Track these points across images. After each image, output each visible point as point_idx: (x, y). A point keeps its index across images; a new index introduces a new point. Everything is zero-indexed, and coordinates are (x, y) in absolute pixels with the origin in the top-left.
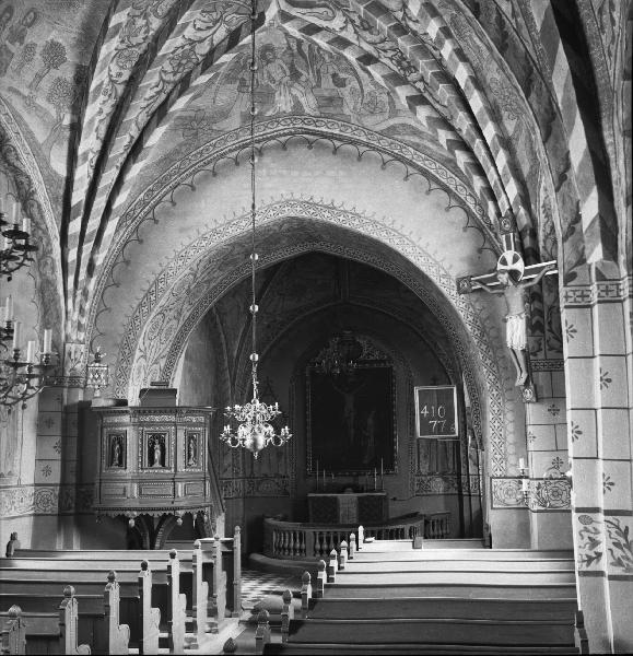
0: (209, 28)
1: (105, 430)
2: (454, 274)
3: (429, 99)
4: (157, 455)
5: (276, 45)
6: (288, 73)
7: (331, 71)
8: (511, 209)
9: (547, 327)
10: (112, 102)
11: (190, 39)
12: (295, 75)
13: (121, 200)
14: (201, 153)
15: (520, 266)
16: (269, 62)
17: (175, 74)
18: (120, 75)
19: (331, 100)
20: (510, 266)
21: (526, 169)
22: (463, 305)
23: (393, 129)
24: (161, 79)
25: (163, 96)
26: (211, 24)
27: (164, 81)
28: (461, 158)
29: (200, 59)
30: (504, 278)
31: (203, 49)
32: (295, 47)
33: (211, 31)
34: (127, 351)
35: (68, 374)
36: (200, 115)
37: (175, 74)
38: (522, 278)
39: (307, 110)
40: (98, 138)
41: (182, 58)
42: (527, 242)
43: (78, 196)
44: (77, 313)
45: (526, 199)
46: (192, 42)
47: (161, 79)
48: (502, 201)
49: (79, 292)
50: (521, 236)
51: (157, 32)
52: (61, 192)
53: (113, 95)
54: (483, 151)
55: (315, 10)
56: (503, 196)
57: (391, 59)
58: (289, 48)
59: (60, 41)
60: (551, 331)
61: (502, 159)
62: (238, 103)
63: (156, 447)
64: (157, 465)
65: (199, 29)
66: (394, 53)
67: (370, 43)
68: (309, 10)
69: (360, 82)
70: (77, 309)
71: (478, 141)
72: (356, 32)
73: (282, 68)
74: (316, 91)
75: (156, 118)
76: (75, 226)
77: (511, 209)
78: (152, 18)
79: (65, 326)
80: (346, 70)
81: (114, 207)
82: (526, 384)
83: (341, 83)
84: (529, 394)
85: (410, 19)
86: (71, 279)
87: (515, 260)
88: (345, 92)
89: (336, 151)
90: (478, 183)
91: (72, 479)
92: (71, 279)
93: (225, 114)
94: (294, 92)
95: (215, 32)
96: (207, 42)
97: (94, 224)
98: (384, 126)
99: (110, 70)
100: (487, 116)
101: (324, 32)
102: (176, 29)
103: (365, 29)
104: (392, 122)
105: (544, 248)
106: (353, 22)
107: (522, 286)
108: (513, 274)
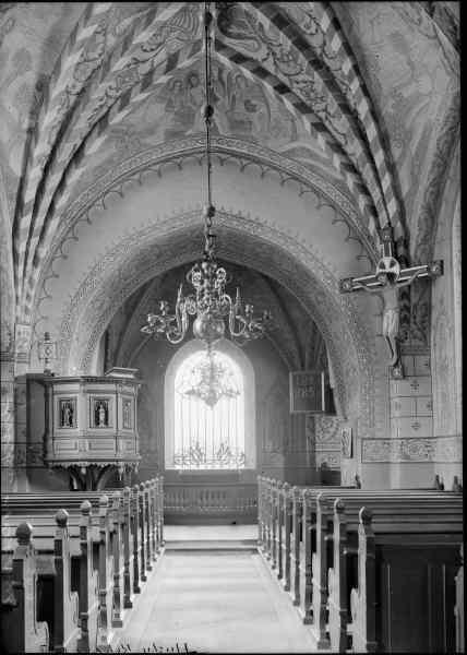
0: (152, 50)
1: (56, 397)
2: (337, 276)
3: (330, 128)
4: (102, 417)
7: (244, 98)
8: (389, 223)
9: (412, 320)
10: (64, 111)
13: (62, 202)
15: (396, 269)
20: (388, 270)
21: (405, 189)
22: (344, 302)
23: (293, 151)
24: (106, 94)
25: (105, 110)
26: (154, 47)
28: (350, 180)
29: (141, 77)
30: (383, 279)
34: (66, 333)
35: (17, 351)
38: (397, 279)
40: (49, 142)
42: (401, 251)
43: (30, 195)
44: (25, 298)
45: (402, 214)
46: (137, 62)
47: (106, 94)
48: (382, 216)
49: (26, 280)
50: (395, 246)
52: (16, 191)
54: (371, 174)
56: (384, 212)
57: (301, 90)
60: (415, 323)
61: (386, 181)
63: (100, 413)
64: (102, 425)
65: (145, 51)
67: (285, 75)
70: (25, 295)
71: (368, 165)
72: (275, 63)
75: (97, 130)
76: (25, 222)
77: (389, 223)
78: (109, 36)
79: (16, 310)
81: (57, 207)
82: (396, 365)
83: (250, 108)
84: (397, 372)
86: (21, 268)
87: (392, 265)
90: (362, 202)
91: (23, 439)
92: (21, 268)
93: (151, 132)
96: (148, 63)
97: (40, 221)
100: (378, 144)
101: (248, 62)
104: (294, 145)
105: (416, 256)
106: (274, 54)
107: (398, 285)
108: (391, 276)
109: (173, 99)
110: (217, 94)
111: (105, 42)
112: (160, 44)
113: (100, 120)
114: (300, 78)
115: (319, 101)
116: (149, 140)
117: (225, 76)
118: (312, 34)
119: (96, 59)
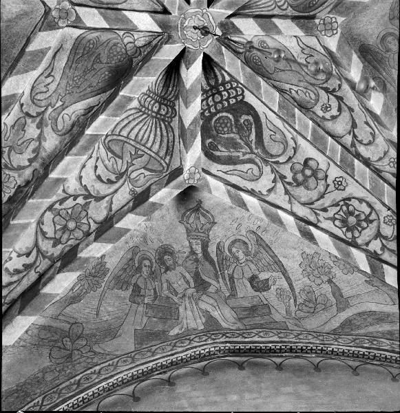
0: (110, 182)
5: (176, 247)
6: (192, 285)
12: (201, 285)
14: (79, 383)
16: (167, 269)
17: (57, 242)
19: (253, 310)
23: (348, 323)
24: (36, 245)
25: (33, 276)
26: (113, 178)
27: (39, 251)
29: (93, 226)
31: (98, 212)
32: (198, 249)
37: (57, 242)
39: (224, 325)
41: (71, 218)
47: (36, 245)
51: (49, 156)
55: (239, 167)
57: (333, 219)
58: (193, 252)
62: (131, 318)
65: (99, 177)
67: (304, 204)
68: (231, 167)
69: (288, 279)
72: (287, 192)
73: (185, 277)
74: (232, 302)
75: (18, 305)
78: (48, 130)
80: (268, 268)
85: (360, 142)
88: (271, 296)
89: (279, 367)
93: (111, 332)
94: (203, 306)
95: (116, 191)
96: (104, 203)
98: (335, 324)
102: (82, 142)
103: (299, 185)
104: (344, 316)
106: (283, 177)
109: (141, 283)
110: (207, 279)
111: (40, 138)
112: (120, 175)
113: (23, 294)
114: (327, 201)
115: (364, 224)
116: (110, 346)
117: (212, 250)
118: (334, 118)
119: (20, 168)
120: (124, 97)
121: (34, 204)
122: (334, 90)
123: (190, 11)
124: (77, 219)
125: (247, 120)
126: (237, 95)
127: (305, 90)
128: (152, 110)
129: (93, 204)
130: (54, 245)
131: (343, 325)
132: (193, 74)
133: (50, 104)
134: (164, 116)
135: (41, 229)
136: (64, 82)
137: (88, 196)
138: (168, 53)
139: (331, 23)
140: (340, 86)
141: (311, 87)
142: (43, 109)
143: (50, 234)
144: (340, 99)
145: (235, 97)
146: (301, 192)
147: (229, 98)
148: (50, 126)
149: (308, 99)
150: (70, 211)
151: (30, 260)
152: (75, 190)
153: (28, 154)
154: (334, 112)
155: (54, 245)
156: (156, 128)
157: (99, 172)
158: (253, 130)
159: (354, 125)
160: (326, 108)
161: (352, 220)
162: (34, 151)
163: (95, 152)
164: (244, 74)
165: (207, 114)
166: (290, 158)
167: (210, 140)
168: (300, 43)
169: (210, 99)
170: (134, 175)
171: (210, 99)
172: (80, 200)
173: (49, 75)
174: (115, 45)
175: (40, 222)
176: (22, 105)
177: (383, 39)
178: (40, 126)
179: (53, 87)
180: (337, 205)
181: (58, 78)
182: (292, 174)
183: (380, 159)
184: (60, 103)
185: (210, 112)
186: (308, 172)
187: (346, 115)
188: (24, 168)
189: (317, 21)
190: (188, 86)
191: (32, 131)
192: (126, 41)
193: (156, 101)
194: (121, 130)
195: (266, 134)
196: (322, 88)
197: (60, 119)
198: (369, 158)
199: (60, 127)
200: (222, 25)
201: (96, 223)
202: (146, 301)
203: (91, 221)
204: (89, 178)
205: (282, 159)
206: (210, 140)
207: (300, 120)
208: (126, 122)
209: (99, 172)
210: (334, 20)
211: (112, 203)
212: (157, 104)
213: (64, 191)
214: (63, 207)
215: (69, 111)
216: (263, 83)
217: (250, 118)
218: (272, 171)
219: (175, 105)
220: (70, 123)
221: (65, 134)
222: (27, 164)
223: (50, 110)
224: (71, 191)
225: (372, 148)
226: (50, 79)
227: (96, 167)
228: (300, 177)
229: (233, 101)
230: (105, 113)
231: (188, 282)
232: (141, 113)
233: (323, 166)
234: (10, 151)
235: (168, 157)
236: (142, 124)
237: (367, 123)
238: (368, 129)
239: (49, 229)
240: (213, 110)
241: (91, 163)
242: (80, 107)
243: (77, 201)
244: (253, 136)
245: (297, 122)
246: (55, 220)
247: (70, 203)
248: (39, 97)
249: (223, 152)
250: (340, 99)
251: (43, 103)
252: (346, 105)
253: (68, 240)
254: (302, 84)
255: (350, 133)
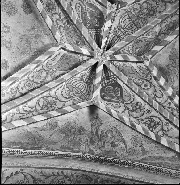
0: (66, 98)
5: (86, 129)
6: (89, 141)
7: (111, 142)
11: (57, 96)
12: (92, 142)
16: (81, 134)
17: (42, 109)
18: (22, 89)
24: (35, 107)
26: (67, 97)
27: (36, 109)
32: (94, 132)
33: (66, 100)
36: (40, 138)
41: (49, 103)
47: (35, 107)
53: (14, 95)
55: (112, 103)
57: (145, 123)
58: (92, 132)
59: (10, 63)
62: (61, 142)
65: (62, 95)
66: (147, 120)
67: (135, 118)
68: (110, 103)
69: (125, 145)
72: (129, 113)
73: (86, 138)
74: (102, 149)
78: (49, 76)
80: (118, 140)
85: (157, 97)
88: (117, 149)
95: (67, 101)
96: (62, 103)
99: (20, 83)
103: (134, 111)
104: (144, 157)
106: (128, 108)
109: (69, 134)
110: (94, 140)
111: (46, 77)
112: (70, 97)
114: (144, 117)
115: (157, 125)
117: (99, 133)
118: (148, 89)
119: (37, 83)
120: (75, 70)
121: (37, 91)
122: (149, 80)
123: (101, 51)
124: (51, 104)
125: (118, 89)
126: (115, 80)
127: (139, 80)
128: (85, 81)
129: (58, 102)
130: (41, 109)
131: (142, 159)
132: (100, 69)
133: (52, 69)
134: (89, 83)
135: (38, 103)
136: (58, 64)
137: (57, 99)
138: (93, 62)
139: (147, 57)
140: (151, 79)
141: (141, 79)
142: (49, 69)
143: (41, 105)
144: (151, 83)
145: (114, 81)
146: (135, 114)
147: (112, 81)
148: (50, 75)
149: (140, 83)
150: (49, 101)
151: (32, 110)
152: (53, 95)
153: (41, 80)
154: (149, 87)
155: (41, 109)
156: (86, 86)
157: (62, 93)
158: (120, 93)
159: (155, 91)
160: (145, 86)
161: (152, 124)
162: (43, 80)
163: (63, 87)
164: (116, 71)
165: (104, 85)
166: (132, 102)
167: (104, 93)
168: (138, 66)
169: (106, 81)
170: (75, 98)
171: (106, 81)
172: (54, 99)
173: (53, 60)
174: (76, 58)
175: (39, 100)
176: (43, 66)
177: (168, 66)
178: (47, 73)
179: (54, 64)
180: (147, 119)
181: (56, 62)
182: (132, 108)
183: (164, 103)
184: (55, 69)
185: (105, 85)
186: (138, 107)
187: (153, 88)
188: (38, 83)
189: (142, 57)
190: (97, 73)
191: (44, 74)
192: (80, 58)
193: (87, 78)
194: (73, 83)
195: (124, 93)
196: (145, 80)
197: (54, 74)
198: (160, 102)
199: (53, 76)
200: (110, 56)
201: (57, 107)
202: (69, 139)
203: (56, 107)
204: (59, 93)
205: (129, 102)
206: (104, 93)
207: (134, 86)
208: (75, 81)
209: (62, 93)
210: (148, 56)
211: (65, 104)
212: (87, 79)
213: (49, 94)
214: (47, 99)
215: (57, 72)
216: (122, 74)
217: (119, 88)
218: (125, 106)
219: (93, 80)
220: (57, 75)
221: (54, 78)
222: (40, 82)
223: (51, 70)
224: (52, 95)
225: (161, 99)
226: (53, 62)
227: (62, 91)
228: (134, 109)
229: (113, 82)
230: (68, 73)
231: (87, 140)
232: (82, 81)
233: (143, 105)
234: (36, 78)
235: (88, 96)
236: (81, 84)
237: (160, 91)
238: (160, 93)
239: (41, 103)
240: (106, 84)
241: (61, 89)
242: (61, 72)
243: (53, 99)
244: (119, 94)
245: (133, 87)
246: (44, 102)
247: (50, 98)
248: (49, 65)
249: (107, 98)
250: (151, 83)
251: (50, 68)
252: (153, 85)
253: (46, 110)
254: (138, 78)
255: (154, 94)
